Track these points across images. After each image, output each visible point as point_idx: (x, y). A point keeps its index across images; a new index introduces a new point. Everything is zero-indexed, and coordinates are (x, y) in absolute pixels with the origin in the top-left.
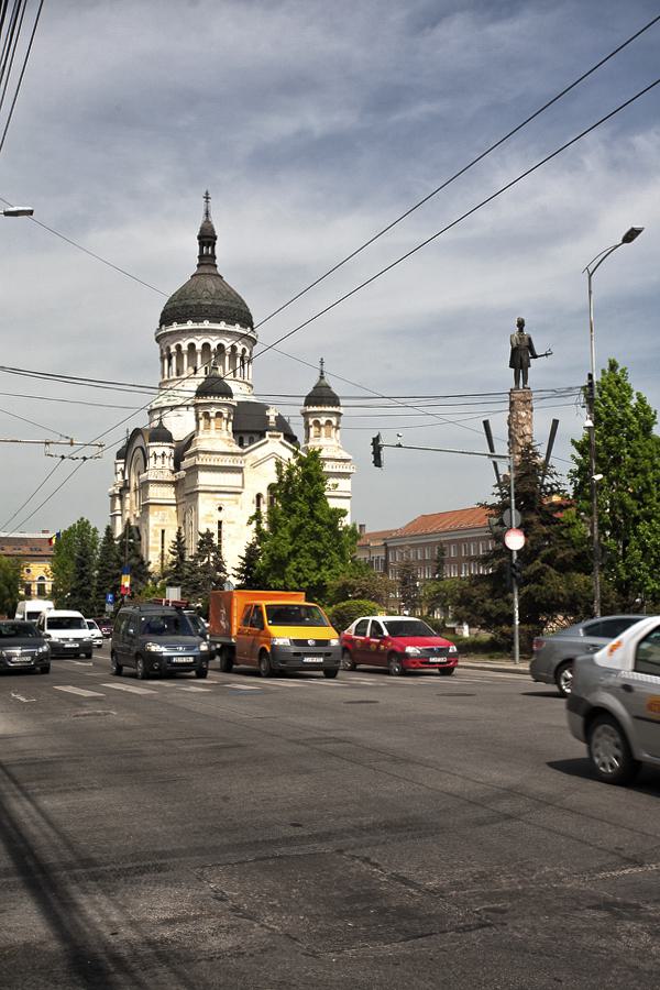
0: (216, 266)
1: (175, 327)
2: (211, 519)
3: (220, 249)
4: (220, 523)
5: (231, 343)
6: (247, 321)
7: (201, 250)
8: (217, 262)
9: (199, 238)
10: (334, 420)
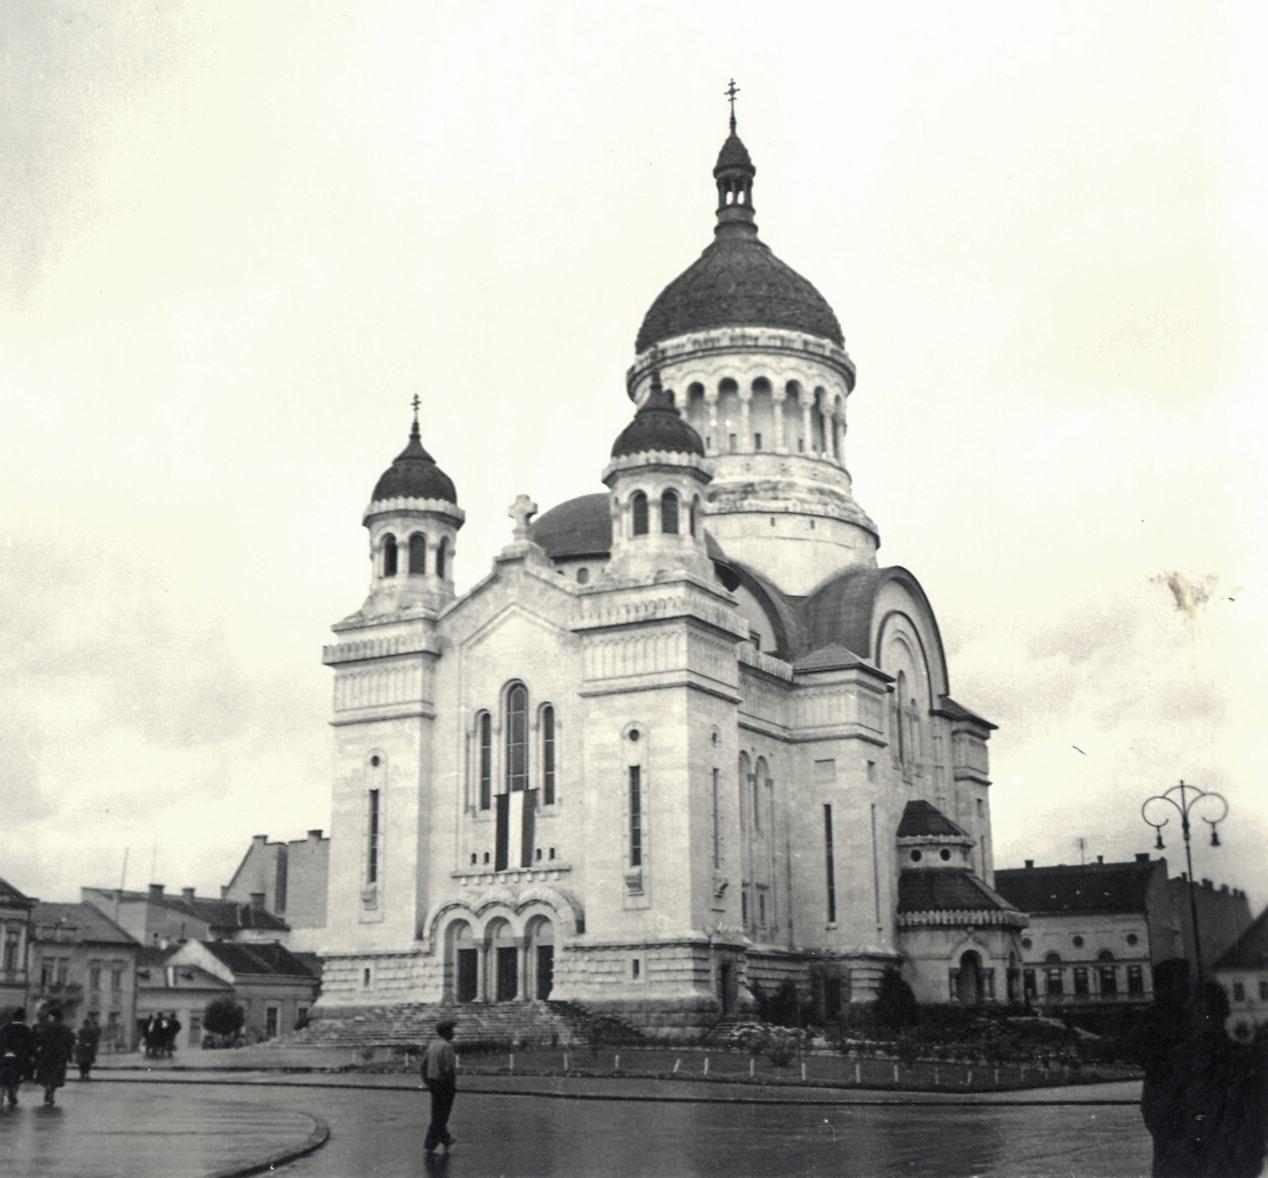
0: (755, 228)
4: (375, 794)
5: (818, 382)
6: (819, 319)
7: (722, 199)
8: (757, 220)
9: (716, 172)
10: (686, 490)
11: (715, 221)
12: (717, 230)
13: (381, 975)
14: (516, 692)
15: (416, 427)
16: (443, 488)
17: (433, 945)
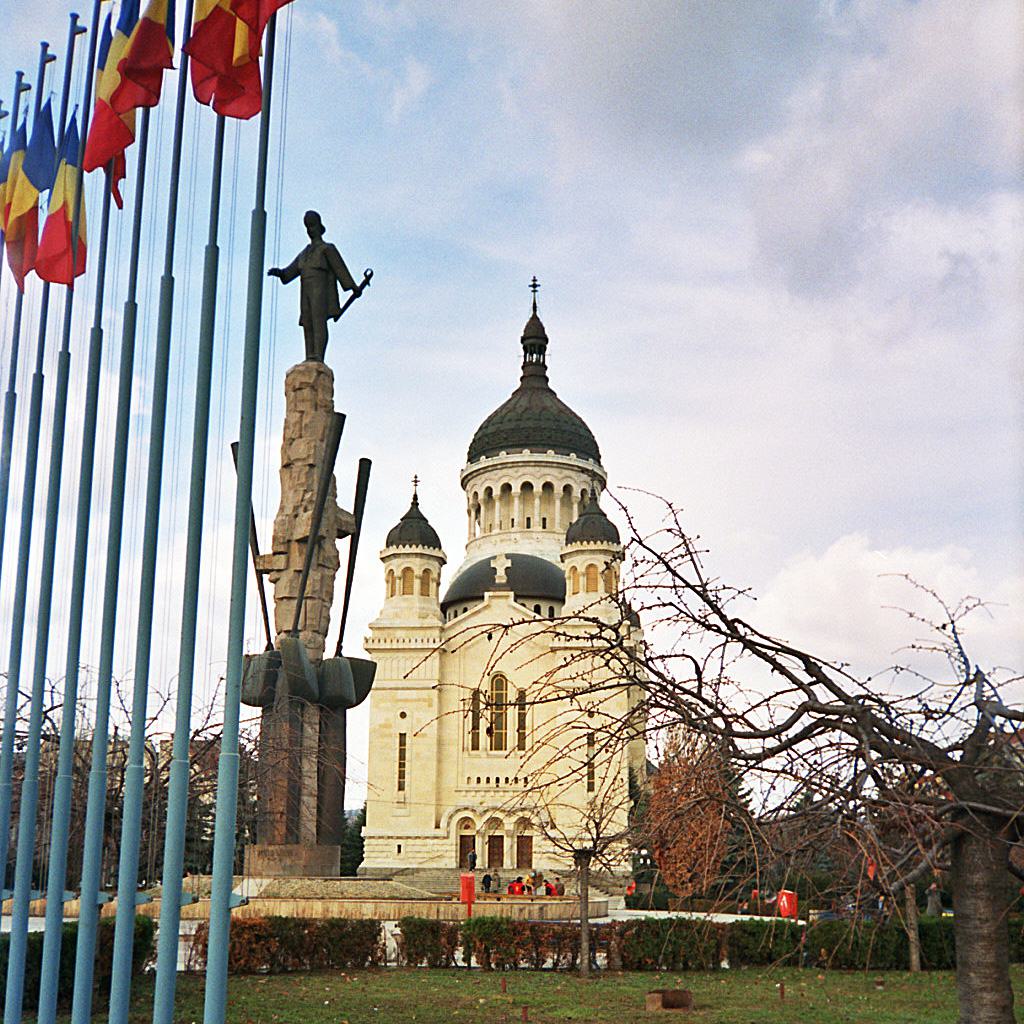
0: (547, 379)
1: (484, 462)
2: (387, 731)
3: (553, 358)
4: (403, 736)
8: (548, 374)
11: (521, 373)
12: (522, 379)
13: (409, 849)
14: (499, 681)
15: (415, 497)
16: (432, 539)
17: (448, 833)
